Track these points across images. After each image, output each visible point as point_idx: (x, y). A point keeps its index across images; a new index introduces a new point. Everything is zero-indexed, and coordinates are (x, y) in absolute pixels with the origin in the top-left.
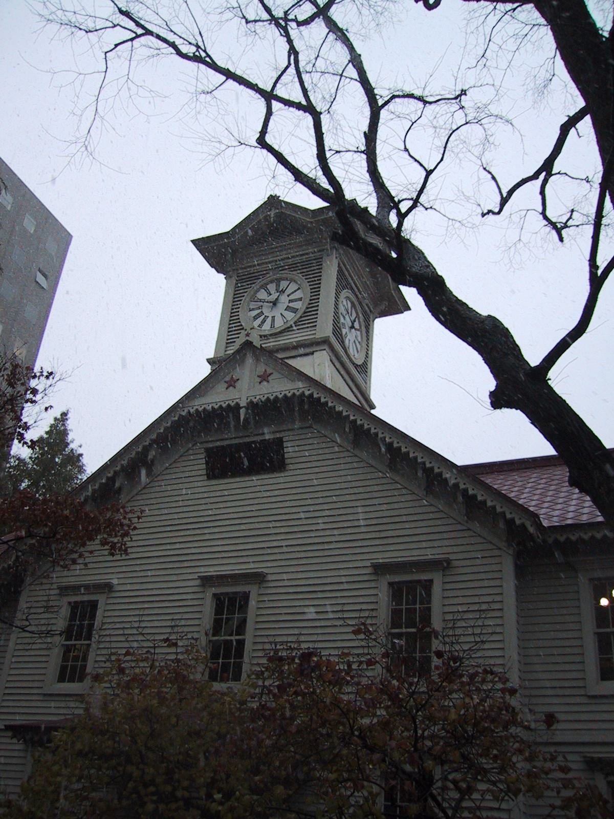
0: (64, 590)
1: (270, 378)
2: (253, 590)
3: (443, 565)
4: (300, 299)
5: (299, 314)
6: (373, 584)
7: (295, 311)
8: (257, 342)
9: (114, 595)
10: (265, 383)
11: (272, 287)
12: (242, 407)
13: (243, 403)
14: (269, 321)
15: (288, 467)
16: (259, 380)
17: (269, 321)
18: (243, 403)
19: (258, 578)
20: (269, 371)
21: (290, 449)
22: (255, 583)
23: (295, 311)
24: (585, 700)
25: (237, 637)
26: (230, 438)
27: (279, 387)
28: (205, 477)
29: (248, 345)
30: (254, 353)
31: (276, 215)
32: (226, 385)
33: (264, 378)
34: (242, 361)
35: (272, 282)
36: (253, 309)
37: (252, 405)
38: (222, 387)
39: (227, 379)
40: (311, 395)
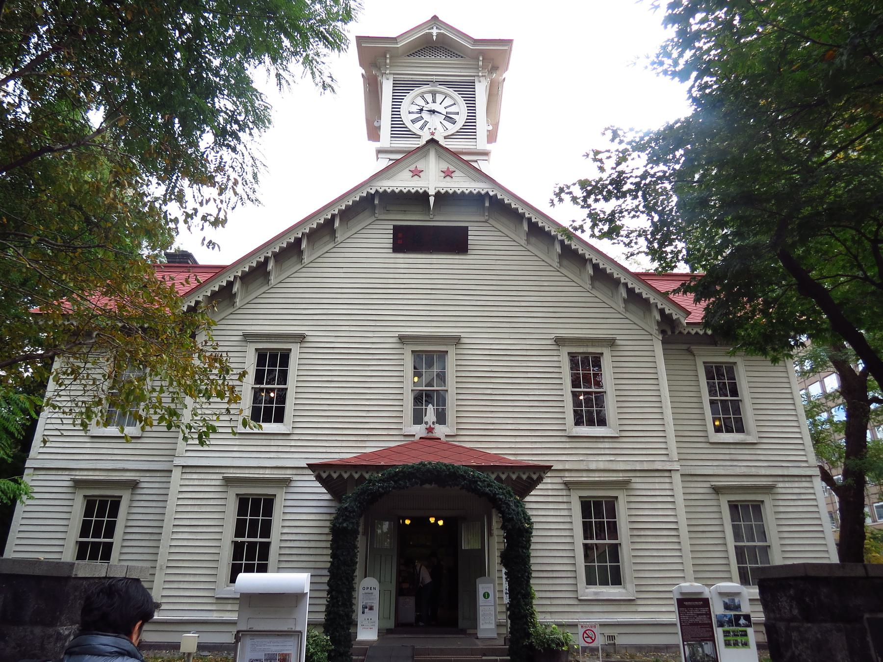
0: (248, 338)
1: (453, 175)
3: (611, 343)
4: (458, 113)
6: (555, 353)
7: (454, 122)
8: (442, 142)
10: (448, 178)
11: (429, 97)
12: (432, 195)
13: (432, 192)
15: (469, 252)
18: (432, 192)
19: (456, 340)
20: (452, 168)
21: (473, 238)
22: (453, 345)
23: (454, 122)
24: (708, 446)
25: (262, 386)
26: (413, 219)
27: (461, 184)
28: (391, 251)
29: (433, 142)
30: (436, 151)
31: (438, 35)
32: (411, 174)
33: (448, 174)
34: (426, 155)
36: (413, 113)
37: (438, 195)
38: (406, 174)
39: (412, 168)
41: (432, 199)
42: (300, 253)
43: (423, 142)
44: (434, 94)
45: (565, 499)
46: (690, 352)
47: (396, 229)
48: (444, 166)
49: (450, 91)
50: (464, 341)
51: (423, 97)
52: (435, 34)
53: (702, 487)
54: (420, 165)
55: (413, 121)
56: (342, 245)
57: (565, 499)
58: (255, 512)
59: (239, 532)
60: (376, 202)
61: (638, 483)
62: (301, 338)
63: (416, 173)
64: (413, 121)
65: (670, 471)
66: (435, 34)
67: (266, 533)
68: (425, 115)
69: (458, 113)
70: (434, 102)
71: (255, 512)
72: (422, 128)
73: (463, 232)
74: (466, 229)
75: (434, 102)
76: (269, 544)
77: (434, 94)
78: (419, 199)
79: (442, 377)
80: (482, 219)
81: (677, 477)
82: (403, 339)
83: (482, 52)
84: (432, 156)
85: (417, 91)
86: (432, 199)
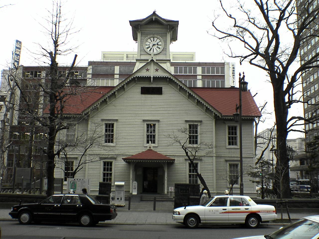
0: (102, 120)
2: (157, 124)
3: (201, 122)
4: (161, 45)
7: (160, 48)
8: (155, 61)
9: (118, 122)
11: (152, 39)
13: (152, 77)
16: (155, 71)
18: (152, 77)
19: (158, 121)
26: (146, 85)
27: (160, 74)
29: (152, 60)
31: (155, 18)
33: (157, 70)
34: (151, 64)
35: (152, 37)
36: (147, 45)
38: (145, 71)
41: (152, 79)
42: (115, 95)
43: (149, 61)
44: (154, 38)
45: (185, 163)
46: (225, 123)
47: (142, 88)
48: (156, 67)
50: (160, 121)
52: (154, 18)
53: (222, 160)
54: (149, 67)
55: (147, 48)
56: (126, 92)
57: (185, 163)
58: (108, 166)
59: (104, 170)
60: (136, 79)
61: (204, 159)
63: (148, 70)
64: (147, 48)
65: (213, 156)
66: (154, 18)
67: (111, 170)
69: (161, 45)
71: (108, 166)
72: (150, 50)
73: (161, 88)
76: (112, 173)
77: (154, 38)
78: (148, 79)
79: (154, 130)
80: (166, 83)
81: (214, 158)
82: (144, 121)
83: (169, 25)
84: (152, 64)
86: (152, 79)
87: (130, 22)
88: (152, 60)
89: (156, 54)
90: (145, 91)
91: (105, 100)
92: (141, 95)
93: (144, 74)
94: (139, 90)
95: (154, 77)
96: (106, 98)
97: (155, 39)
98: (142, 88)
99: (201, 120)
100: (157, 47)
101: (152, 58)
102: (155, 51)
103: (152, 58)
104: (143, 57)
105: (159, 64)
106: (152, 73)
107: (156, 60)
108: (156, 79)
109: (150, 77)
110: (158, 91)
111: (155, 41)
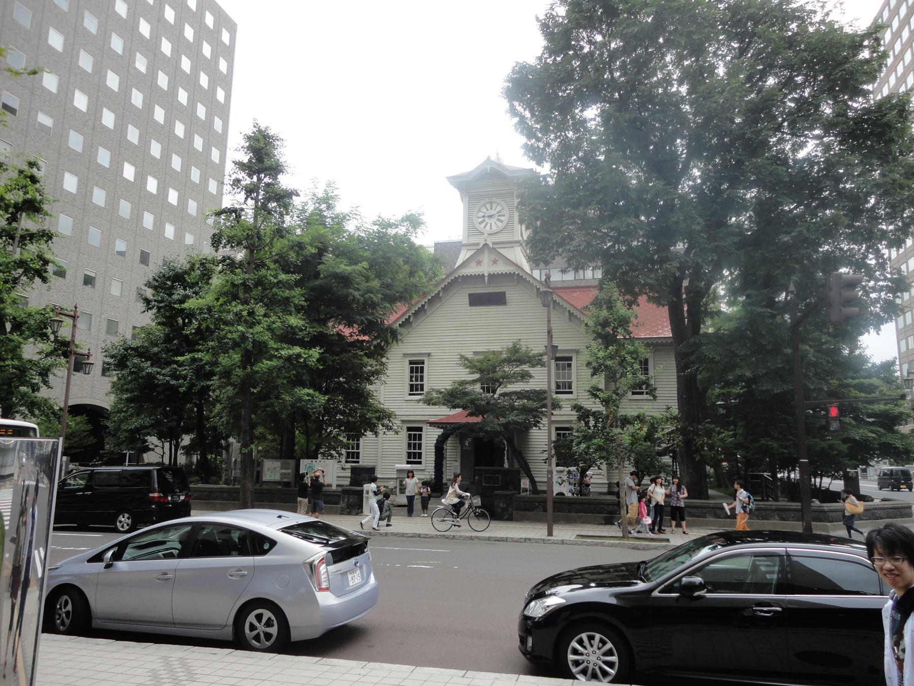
0: (405, 355)
5: (505, 223)
7: (502, 221)
8: (491, 245)
11: (488, 206)
13: (486, 274)
14: (489, 225)
17: (489, 225)
18: (486, 274)
23: (502, 221)
29: (486, 245)
33: (495, 262)
38: (473, 264)
39: (477, 260)
40: (519, 274)
44: (491, 203)
47: (470, 295)
48: (493, 257)
49: (499, 201)
51: (486, 207)
54: (480, 258)
55: (481, 223)
62: (429, 355)
64: (481, 223)
68: (486, 219)
69: (504, 216)
70: (491, 209)
74: (504, 293)
75: (491, 209)
77: (491, 203)
85: (482, 202)
86: (486, 278)
87: (448, 178)
88: (486, 245)
89: (498, 232)
90: (476, 300)
91: (408, 320)
92: (469, 308)
93: (472, 270)
94: (466, 300)
95: (490, 275)
96: (409, 316)
97: (494, 206)
98: (470, 295)
99: (577, 348)
100: (498, 220)
101: (486, 240)
102: (494, 227)
103: (486, 240)
104: (473, 240)
105: (500, 250)
106: (486, 268)
107: (493, 243)
108: (492, 277)
109: (483, 275)
110: (498, 299)
111: (494, 208)
